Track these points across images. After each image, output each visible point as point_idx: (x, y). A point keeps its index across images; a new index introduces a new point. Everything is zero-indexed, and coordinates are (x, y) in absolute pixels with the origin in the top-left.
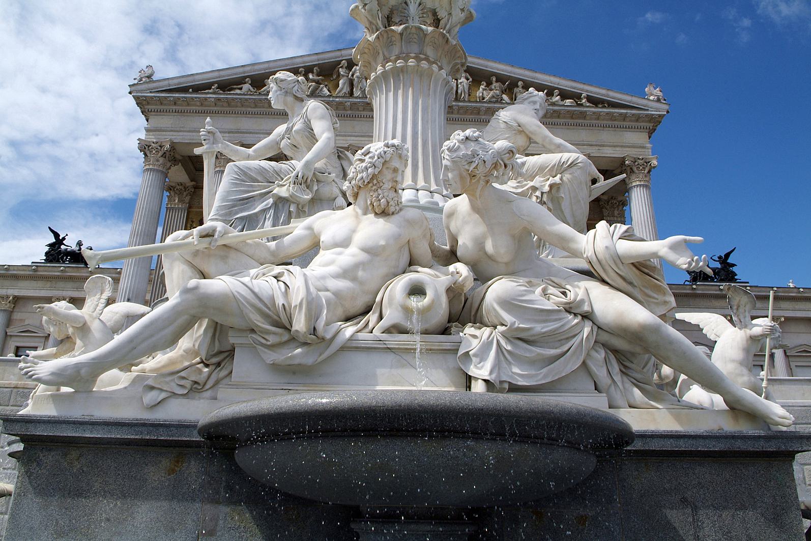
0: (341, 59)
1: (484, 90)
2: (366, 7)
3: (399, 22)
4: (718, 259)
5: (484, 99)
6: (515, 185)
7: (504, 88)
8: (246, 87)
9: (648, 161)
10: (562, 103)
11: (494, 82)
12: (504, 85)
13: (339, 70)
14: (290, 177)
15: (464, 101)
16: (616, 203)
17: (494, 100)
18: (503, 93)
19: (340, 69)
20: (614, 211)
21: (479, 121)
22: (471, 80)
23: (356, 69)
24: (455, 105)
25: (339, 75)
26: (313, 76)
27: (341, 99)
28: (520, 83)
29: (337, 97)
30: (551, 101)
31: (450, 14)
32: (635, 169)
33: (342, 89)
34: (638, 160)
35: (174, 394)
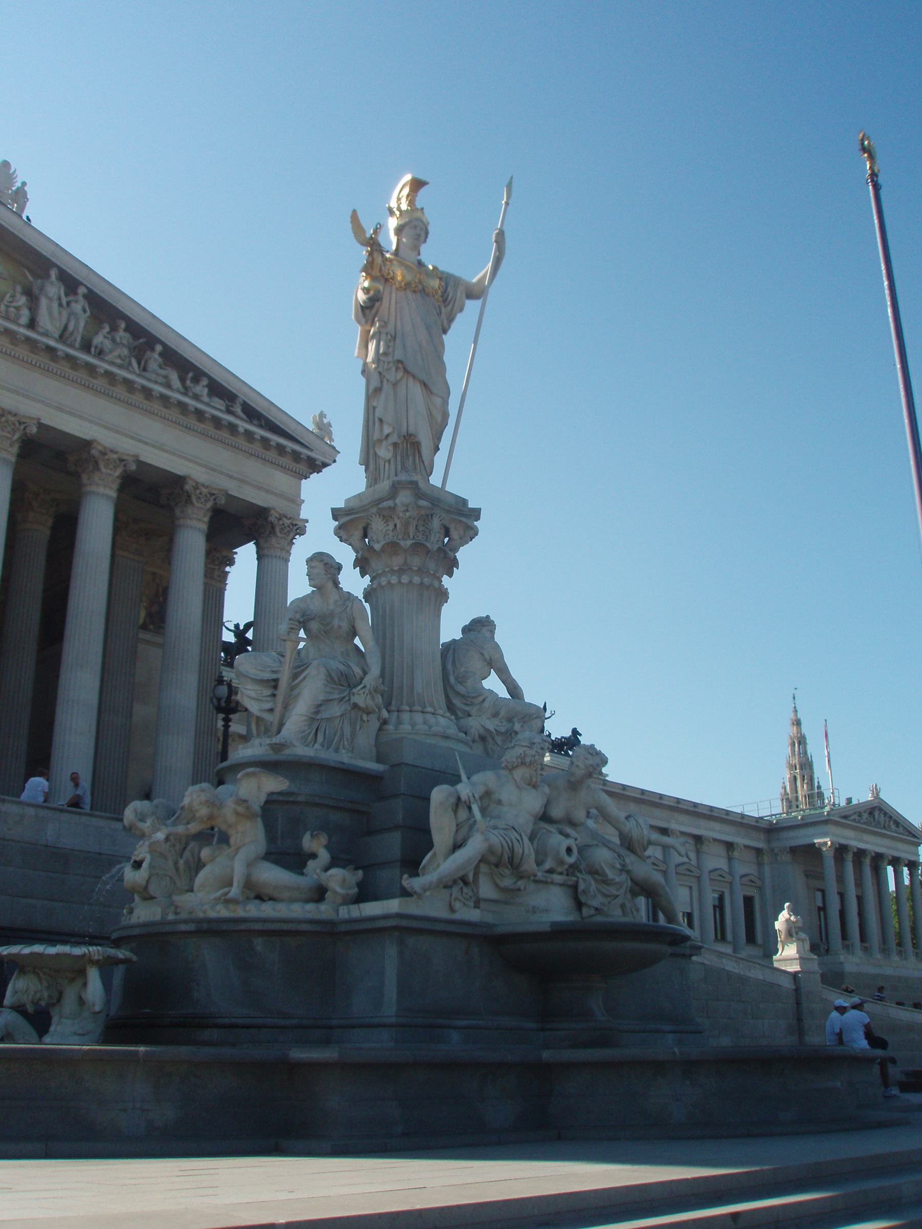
2: (408, 514)
3: (423, 531)
4: (233, 629)
6: (500, 724)
9: (294, 523)
12: (136, 337)
14: (365, 687)
15: (71, 346)
16: (218, 558)
17: (119, 361)
20: (214, 569)
22: (88, 313)
24: (61, 350)
28: (159, 348)
30: (193, 390)
32: (277, 530)
34: (284, 519)
35: (464, 904)
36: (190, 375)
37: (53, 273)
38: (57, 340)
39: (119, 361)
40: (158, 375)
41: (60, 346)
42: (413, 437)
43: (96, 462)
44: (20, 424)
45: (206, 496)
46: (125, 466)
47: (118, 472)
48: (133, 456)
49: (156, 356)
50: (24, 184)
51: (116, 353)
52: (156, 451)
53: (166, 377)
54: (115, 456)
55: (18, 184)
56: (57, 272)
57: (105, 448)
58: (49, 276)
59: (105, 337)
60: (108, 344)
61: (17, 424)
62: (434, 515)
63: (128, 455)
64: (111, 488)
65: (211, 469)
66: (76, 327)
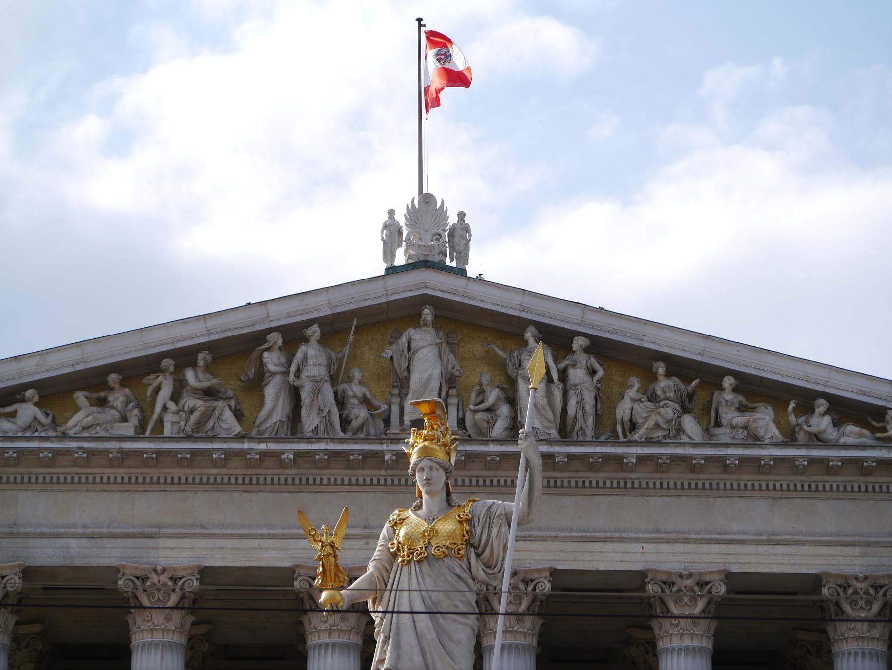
0: (266, 326)
1: (634, 401)
5: (633, 426)
8: (27, 411)
10: (832, 434)
11: (661, 378)
12: (687, 380)
13: (260, 357)
17: (660, 433)
18: (685, 410)
19: (265, 355)
21: (622, 484)
22: (600, 373)
23: (305, 357)
24: (560, 453)
25: (261, 365)
26: (197, 377)
27: (272, 446)
29: (260, 440)
30: (806, 428)
33: (272, 411)
36: (792, 405)
37: (529, 335)
38: (549, 441)
39: (660, 433)
40: (733, 427)
41: (557, 449)
43: (663, 603)
44: (526, 582)
45: (867, 593)
46: (710, 591)
47: (700, 605)
48: (718, 572)
49: (729, 396)
50: (462, 215)
51: (650, 423)
52: (762, 549)
53: (746, 427)
54: (689, 582)
55: (453, 219)
57: (668, 573)
58: (526, 343)
59: (634, 401)
60: (641, 410)
61: (522, 586)
63: (711, 573)
64: (692, 635)
65: (869, 544)
66: (581, 405)
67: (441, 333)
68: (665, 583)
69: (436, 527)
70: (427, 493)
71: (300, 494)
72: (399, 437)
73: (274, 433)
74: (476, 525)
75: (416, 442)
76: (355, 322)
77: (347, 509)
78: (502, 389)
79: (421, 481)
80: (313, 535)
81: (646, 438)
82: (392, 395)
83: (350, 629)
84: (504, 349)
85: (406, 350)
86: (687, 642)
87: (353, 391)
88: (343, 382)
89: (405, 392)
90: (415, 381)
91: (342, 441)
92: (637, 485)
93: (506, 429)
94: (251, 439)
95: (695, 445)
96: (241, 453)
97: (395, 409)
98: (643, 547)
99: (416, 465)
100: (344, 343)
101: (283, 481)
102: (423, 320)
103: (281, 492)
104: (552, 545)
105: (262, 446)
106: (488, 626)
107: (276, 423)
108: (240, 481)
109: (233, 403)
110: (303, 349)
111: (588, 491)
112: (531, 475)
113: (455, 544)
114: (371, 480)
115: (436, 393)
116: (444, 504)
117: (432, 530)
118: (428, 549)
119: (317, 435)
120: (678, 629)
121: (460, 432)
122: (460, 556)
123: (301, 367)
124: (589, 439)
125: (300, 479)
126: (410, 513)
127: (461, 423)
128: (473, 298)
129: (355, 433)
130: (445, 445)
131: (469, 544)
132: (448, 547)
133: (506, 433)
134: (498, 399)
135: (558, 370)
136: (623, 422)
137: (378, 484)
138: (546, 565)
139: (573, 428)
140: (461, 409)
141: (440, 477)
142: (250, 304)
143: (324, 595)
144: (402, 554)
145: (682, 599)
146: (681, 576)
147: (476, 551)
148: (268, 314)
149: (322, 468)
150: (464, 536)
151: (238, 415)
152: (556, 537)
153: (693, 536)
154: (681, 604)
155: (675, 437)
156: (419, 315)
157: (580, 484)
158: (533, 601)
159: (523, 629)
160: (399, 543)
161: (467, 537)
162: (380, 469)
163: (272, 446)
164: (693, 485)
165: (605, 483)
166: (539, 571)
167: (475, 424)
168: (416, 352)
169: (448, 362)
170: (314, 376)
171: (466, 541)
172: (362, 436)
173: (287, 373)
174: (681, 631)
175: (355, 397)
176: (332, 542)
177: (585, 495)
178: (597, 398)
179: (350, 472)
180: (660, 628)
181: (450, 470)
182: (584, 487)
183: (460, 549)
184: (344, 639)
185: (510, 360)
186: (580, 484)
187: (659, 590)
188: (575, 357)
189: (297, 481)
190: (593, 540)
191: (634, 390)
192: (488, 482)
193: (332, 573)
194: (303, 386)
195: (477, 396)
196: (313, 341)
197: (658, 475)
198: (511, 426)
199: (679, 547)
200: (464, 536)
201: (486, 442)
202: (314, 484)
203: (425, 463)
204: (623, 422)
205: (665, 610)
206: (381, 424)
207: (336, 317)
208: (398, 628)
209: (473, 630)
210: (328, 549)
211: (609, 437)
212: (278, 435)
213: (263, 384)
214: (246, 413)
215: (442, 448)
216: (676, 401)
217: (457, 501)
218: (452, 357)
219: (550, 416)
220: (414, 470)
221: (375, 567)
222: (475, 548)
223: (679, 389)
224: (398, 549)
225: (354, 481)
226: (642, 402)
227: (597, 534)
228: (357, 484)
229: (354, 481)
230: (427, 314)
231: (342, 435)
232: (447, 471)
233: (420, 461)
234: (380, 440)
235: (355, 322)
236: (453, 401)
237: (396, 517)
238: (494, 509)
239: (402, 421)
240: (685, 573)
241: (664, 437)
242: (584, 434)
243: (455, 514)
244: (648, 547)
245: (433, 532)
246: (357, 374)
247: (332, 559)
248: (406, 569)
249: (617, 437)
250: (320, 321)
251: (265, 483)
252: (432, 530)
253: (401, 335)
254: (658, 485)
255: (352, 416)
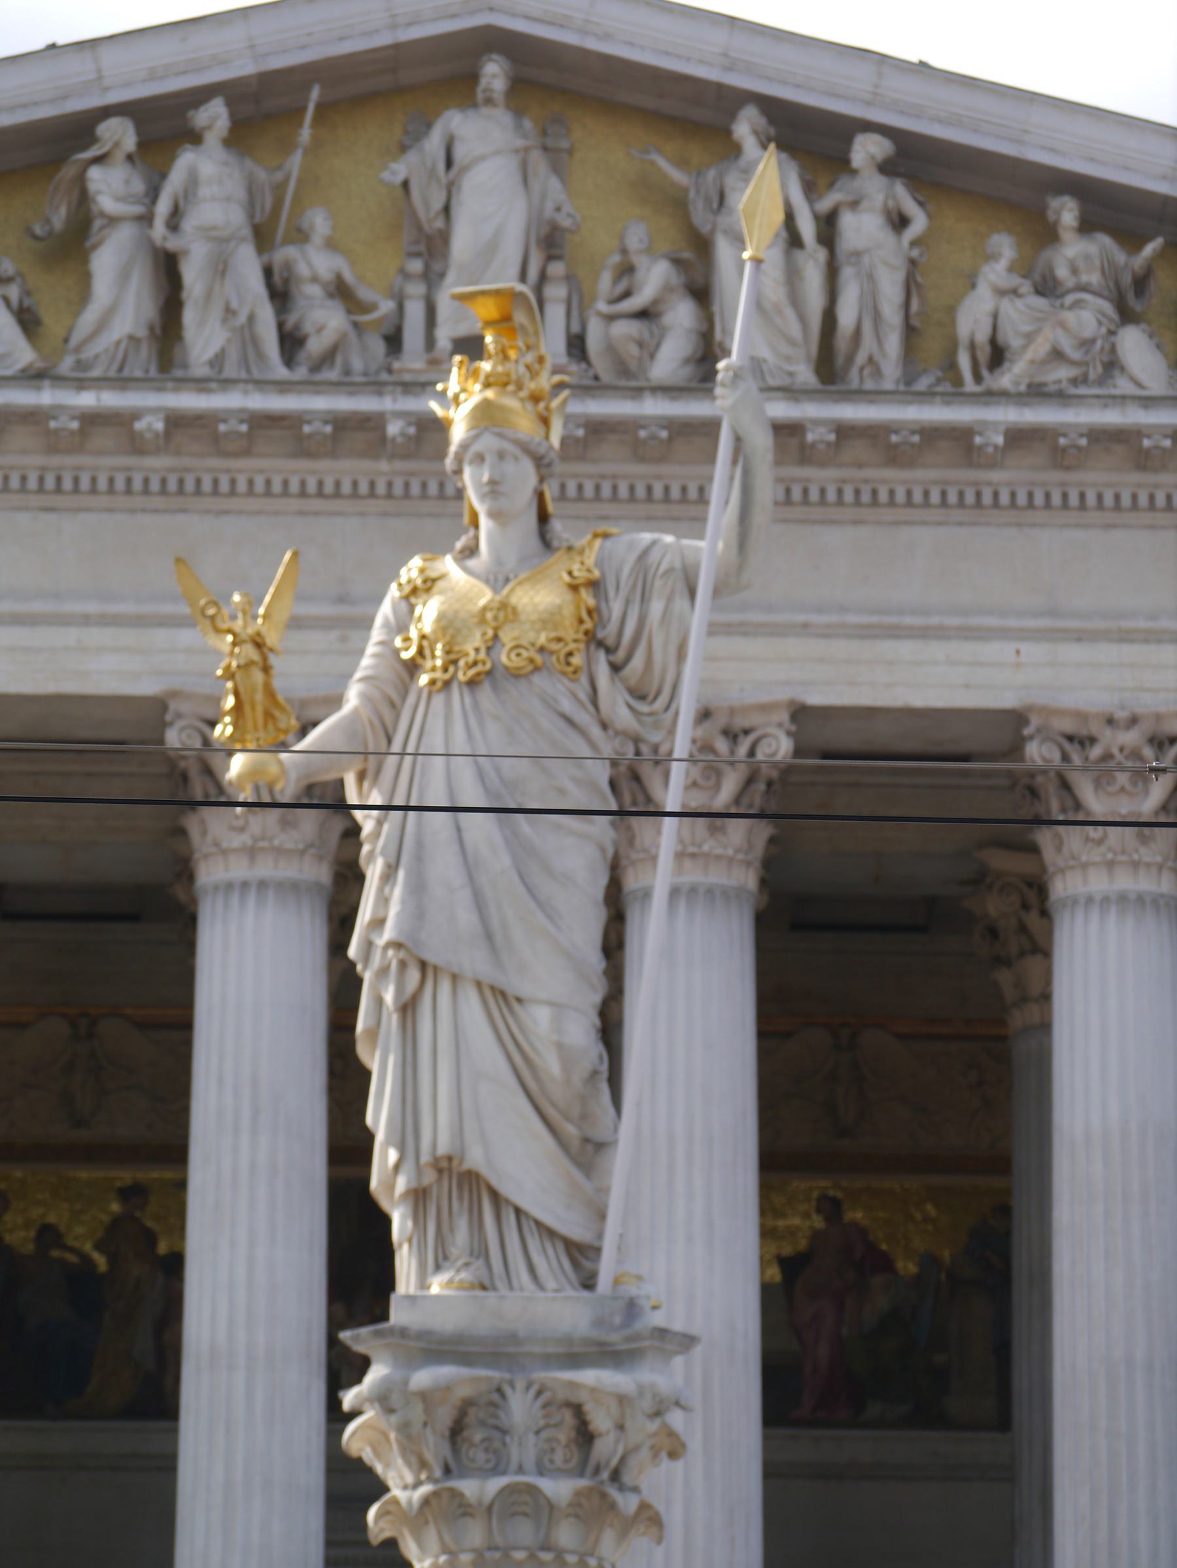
1: (1001, 293)
3: (483, 1441)
5: (998, 355)
7: (1127, 280)
12: (1132, 240)
13: (81, 179)
17: (1062, 374)
18: (1127, 316)
21: (970, 498)
22: (919, 223)
23: (193, 181)
25: (84, 198)
27: (111, 399)
29: (81, 384)
31: (621, 1427)
33: (110, 313)
37: (745, 129)
38: (791, 392)
39: (1062, 374)
42: (455, 1163)
43: (1065, 785)
44: (732, 735)
51: (1040, 348)
56: (761, 121)
57: (1082, 716)
58: (735, 150)
61: (722, 745)
62: (507, 1390)
64: (1135, 865)
67: (528, 124)
68: (1070, 738)
69: (514, 600)
70: (493, 515)
71: (180, 517)
72: (423, 378)
73: (115, 366)
74: (611, 593)
75: (464, 390)
76: (315, 94)
77: (295, 554)
78: (677, 262)
79: (478, 485)
80: (212, 618)
81: (1030, 386)
82: (406, 275)
83: (301, 846)
84: (681, 163)
85: (441, 166)
86: (1124, 882)
87: (310, 264)
88: (287, 241)
89: (437, 267)
90: (462, 243)
91: (283, 387)
92: (1004, 499)
93: (687, 361)
94: (59, 380)
95: (1148, 402)
96: (33, 417)
97: (415, 313)
98: (1018, 652)
99: (464, 446)
100: (287, 146)
101: (137, 484)
102: (485, 91)
103: (132, 511)
104: (794, 646)
105: (87, 400)
106: (637, 842)
107: (118, 343)
108: (32, 484)
109: (13, 292)
110: (186, 160)
111: (887, 514)
112: (746, 473)
113: (559, 640)
114: (355, 484)
115: (514, 270)
116: (534, 542)
117: (503, 606)
118: (494, 653)
119: (220, 371)
120: (1102, 849)
121: (574, 367)
122: (570, 669)
123: (181, 203)
124: (888, 385)
125: (181, 482)
126: (448, 564)
127: (577, 345)
128: (607, 37)
129: (316, 368)
130: (535, 398)
131: (593, 640)
132: (542, 650)
133: (687, 371)
134: (667, 289)
135: (817, 217)
136: (972, 347)
137: (372, 494)
138: (783, 695)
139: (850, 359)
140: (575, 313)
141: (525, 476)
142: (53, 46)
143: (238, 764)
144: (428, 664)
145: (1112, 780)
146: (1110, 721)
147: (612, 658)
148: (99, 71)
149: (236, 455)
150: (581, 621)
151: (28, 321)
152: (805, 626)
153: (1143, 624)
154: (1111, 789)
155: (1101, 381)
156: (472, 78)
157: (866, 497)
158: (750, 781)
159: (725, 847)
160: (423, 637)
161: (588, 625)
162: (376, 457)
163: (111, 399)
164: (1143, 500)
165: (926, 494)
166: (764, 708)
167: (611, 349)
168: (465, 169)
169: (544, 197)
170: (214, 228)
171: (586, 633)
172: (332, 375)
173: (146, 219)
174: (1110, 856)
175: (315, 279)
176: (259, 634)
177: (879, 523)
178: (910, 286)
179: (304, 464)
180: (1059, 848)
181: (546, 461)
182: (875, 502)
183: (570, 654)
184: (289, 871)
185: (698, 192)
186: (866, 497)
187: (1056, 756)
188: (856, 183)
189: (172, 486)
190: (895, 633)
191: (1002, 265)
192: (641, 492)
193: (259, 710)
194: (186, 253)
195: (617, 279)
196: (213, 139)
197: (1056, 476)
198: (699, 354)
199: (1108, 652)
200: (581, 621)
201: (637, 393)
202: (216, 492)
203: (488, 443)
204: (972, 347)
205: (1070, 803)
206: (378, 347)
207: (269, 82)
208: (420, 844)
209: (603, 850)
210: (250, 652)
211: (939, 381)
212: (126, 373)
213: (88, 244)
214: (48, 317)
215: (529, 406)
216: (1106, 293)
217: (565, 535)
218: (554, 183)
219: (795, 329)
220: (459, 459)
221: (365, 697)
222: (609, 651)
223: (1111, 263)
224: (420, 652)
225: (312, 487)
226: (1020, 296)
227: (908, 620)
228: (320, 494)
229: (312, 487)
230: (494, 76)
231: (282, 372)
232: (540, 462)
233: (475, 438)
234: (377, 387)
235: (315, 94)
236: (556, 292)
237: (414, 574)
238: (654, 556)
239: (430, 342)
240: (1121, 715)
241: (1074, 382)
242: (878, 373)
243: (560, 568)
244: (1033, 651)
245: (505, 612)
246: (319, 222)
247: (258, 676)
248: (438, 701)
249: (958, 381)
250: (229, 90)
251: (94, 490)
252: (503, 606)
253: (429, 126)
254: (1056, 499)
255: (308, 327)
